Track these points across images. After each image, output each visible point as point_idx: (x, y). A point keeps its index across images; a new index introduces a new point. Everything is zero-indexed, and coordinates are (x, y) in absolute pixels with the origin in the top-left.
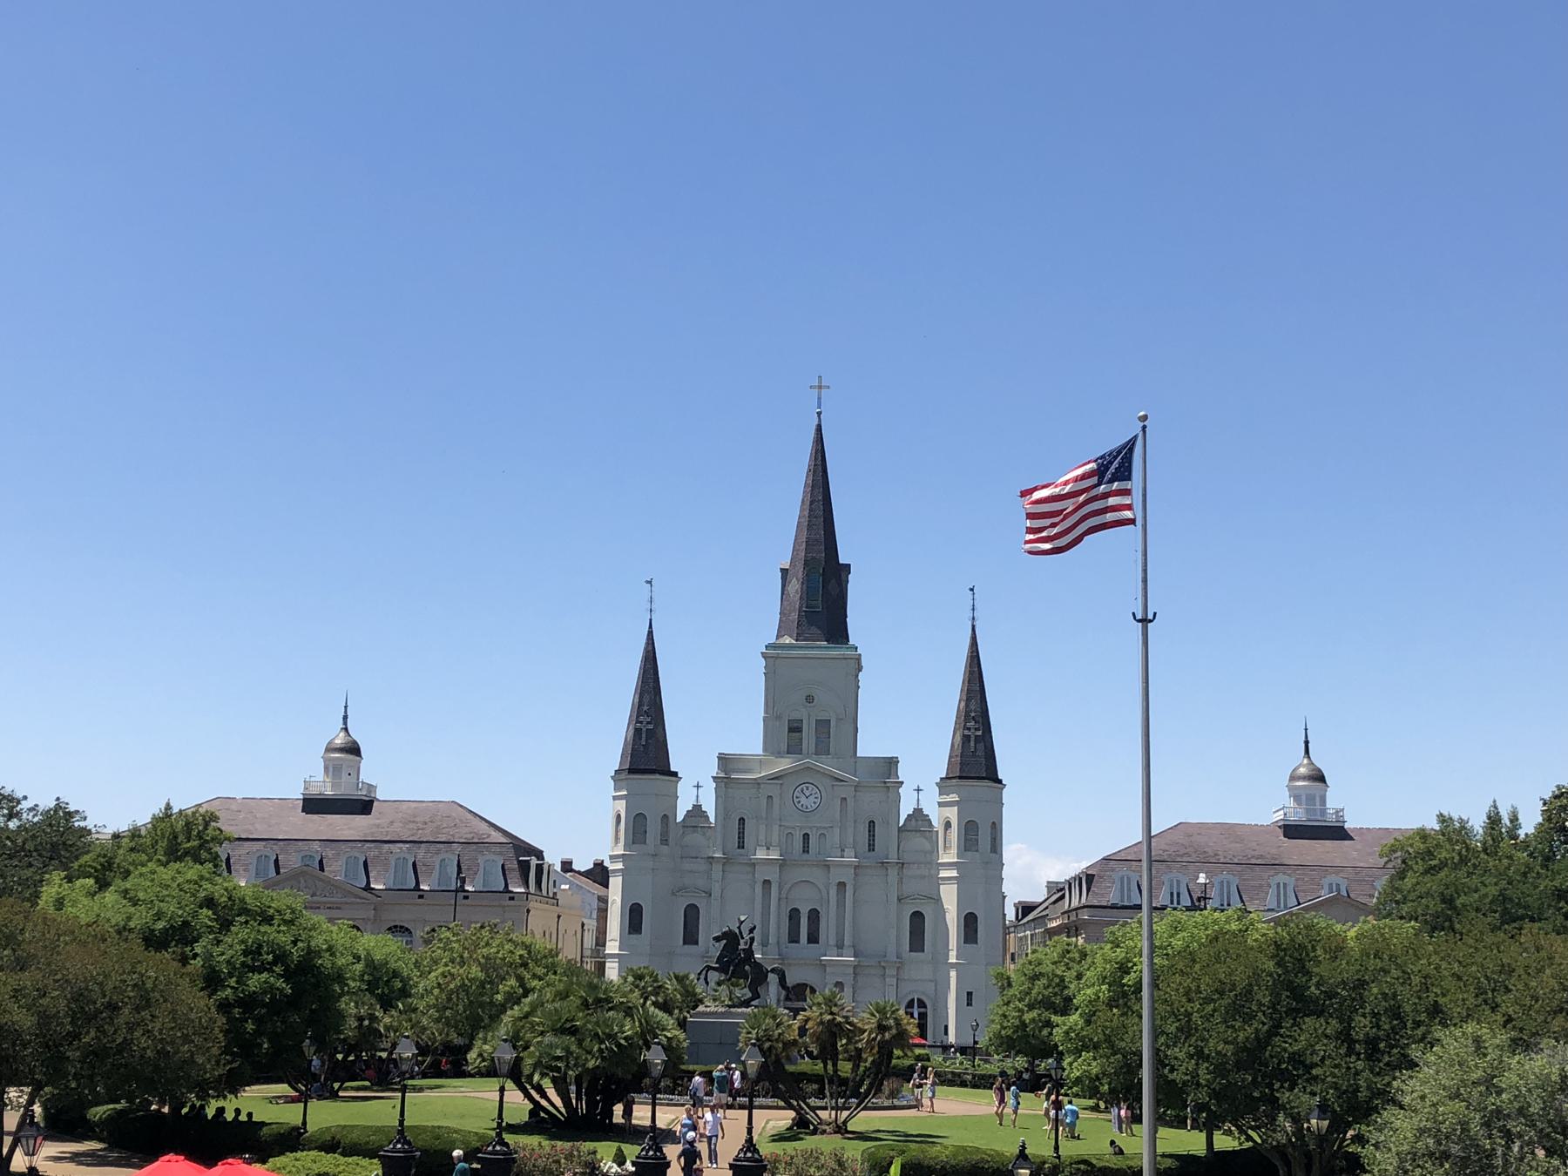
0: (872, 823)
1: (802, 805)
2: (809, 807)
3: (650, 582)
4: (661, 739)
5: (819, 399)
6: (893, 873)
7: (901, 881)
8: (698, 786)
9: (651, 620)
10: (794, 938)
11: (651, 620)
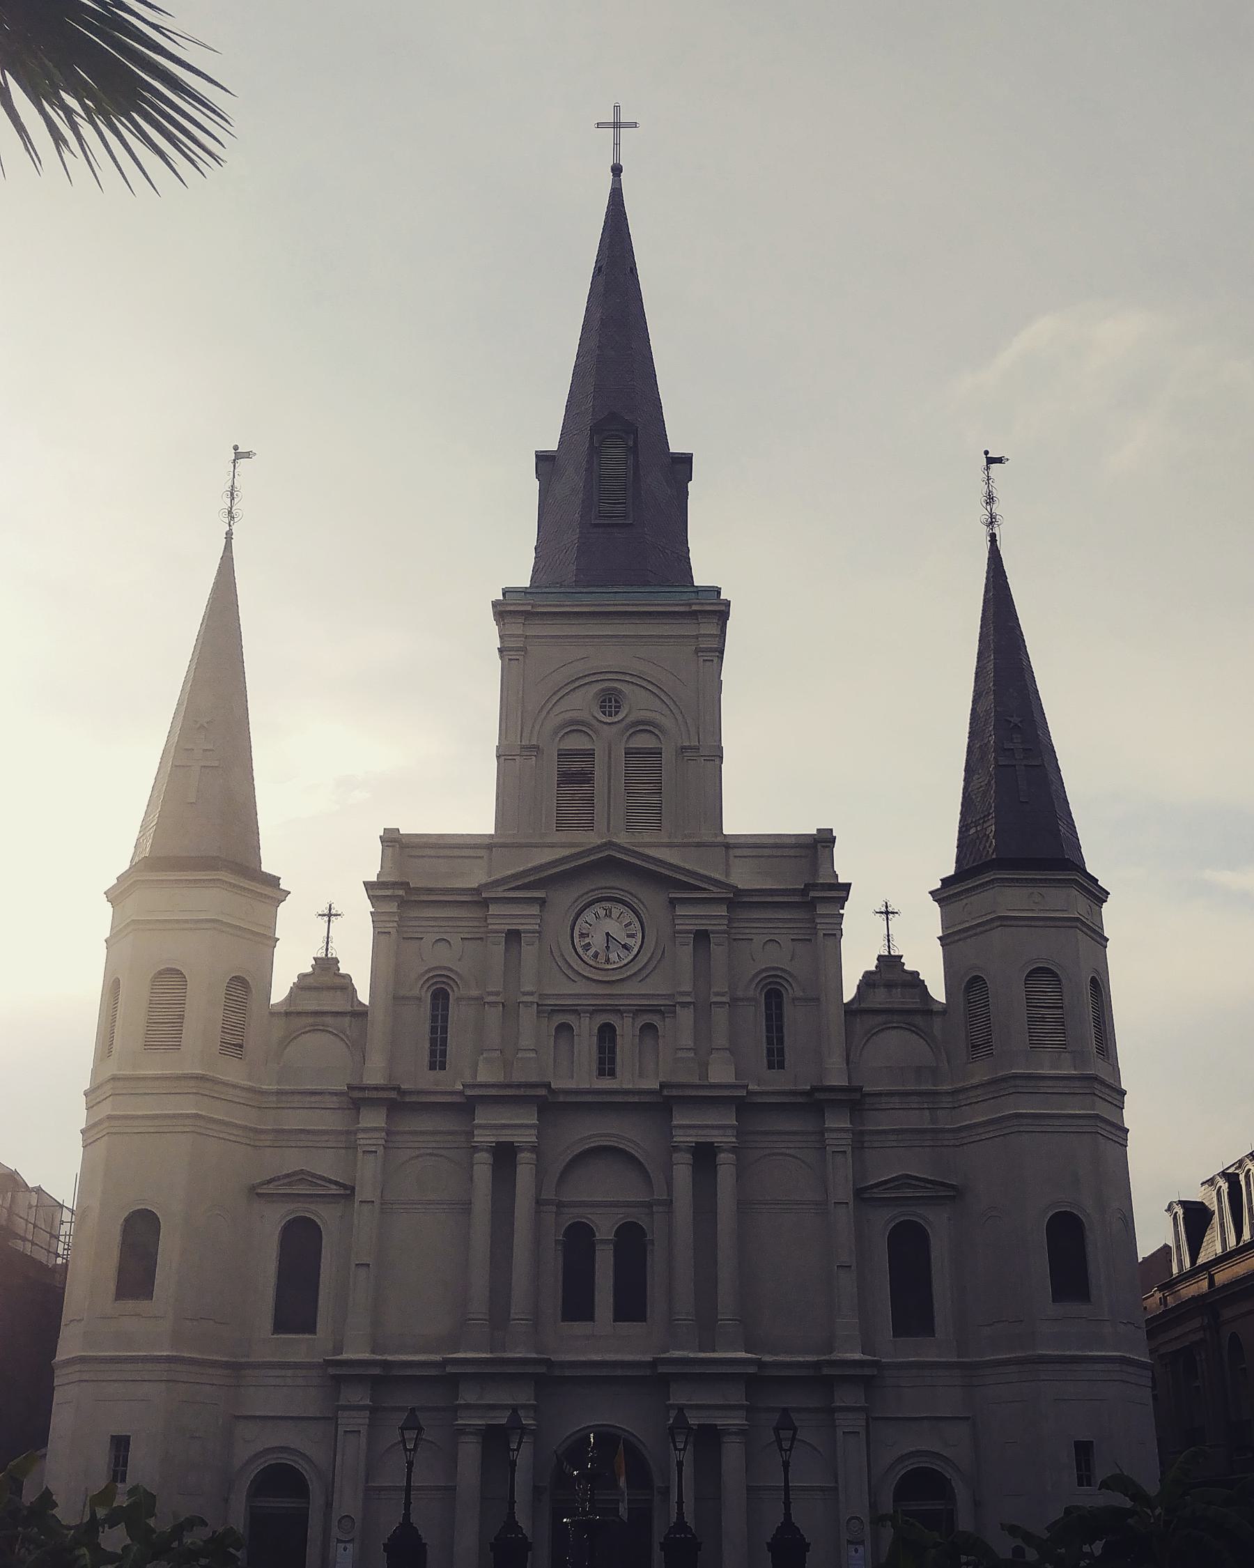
0: (774, 998)
5: (617, 144)
6: (837, 1122)
7: (859, 1142)
8: (330, 915)
9: (229, 536)
11: (229, 536)
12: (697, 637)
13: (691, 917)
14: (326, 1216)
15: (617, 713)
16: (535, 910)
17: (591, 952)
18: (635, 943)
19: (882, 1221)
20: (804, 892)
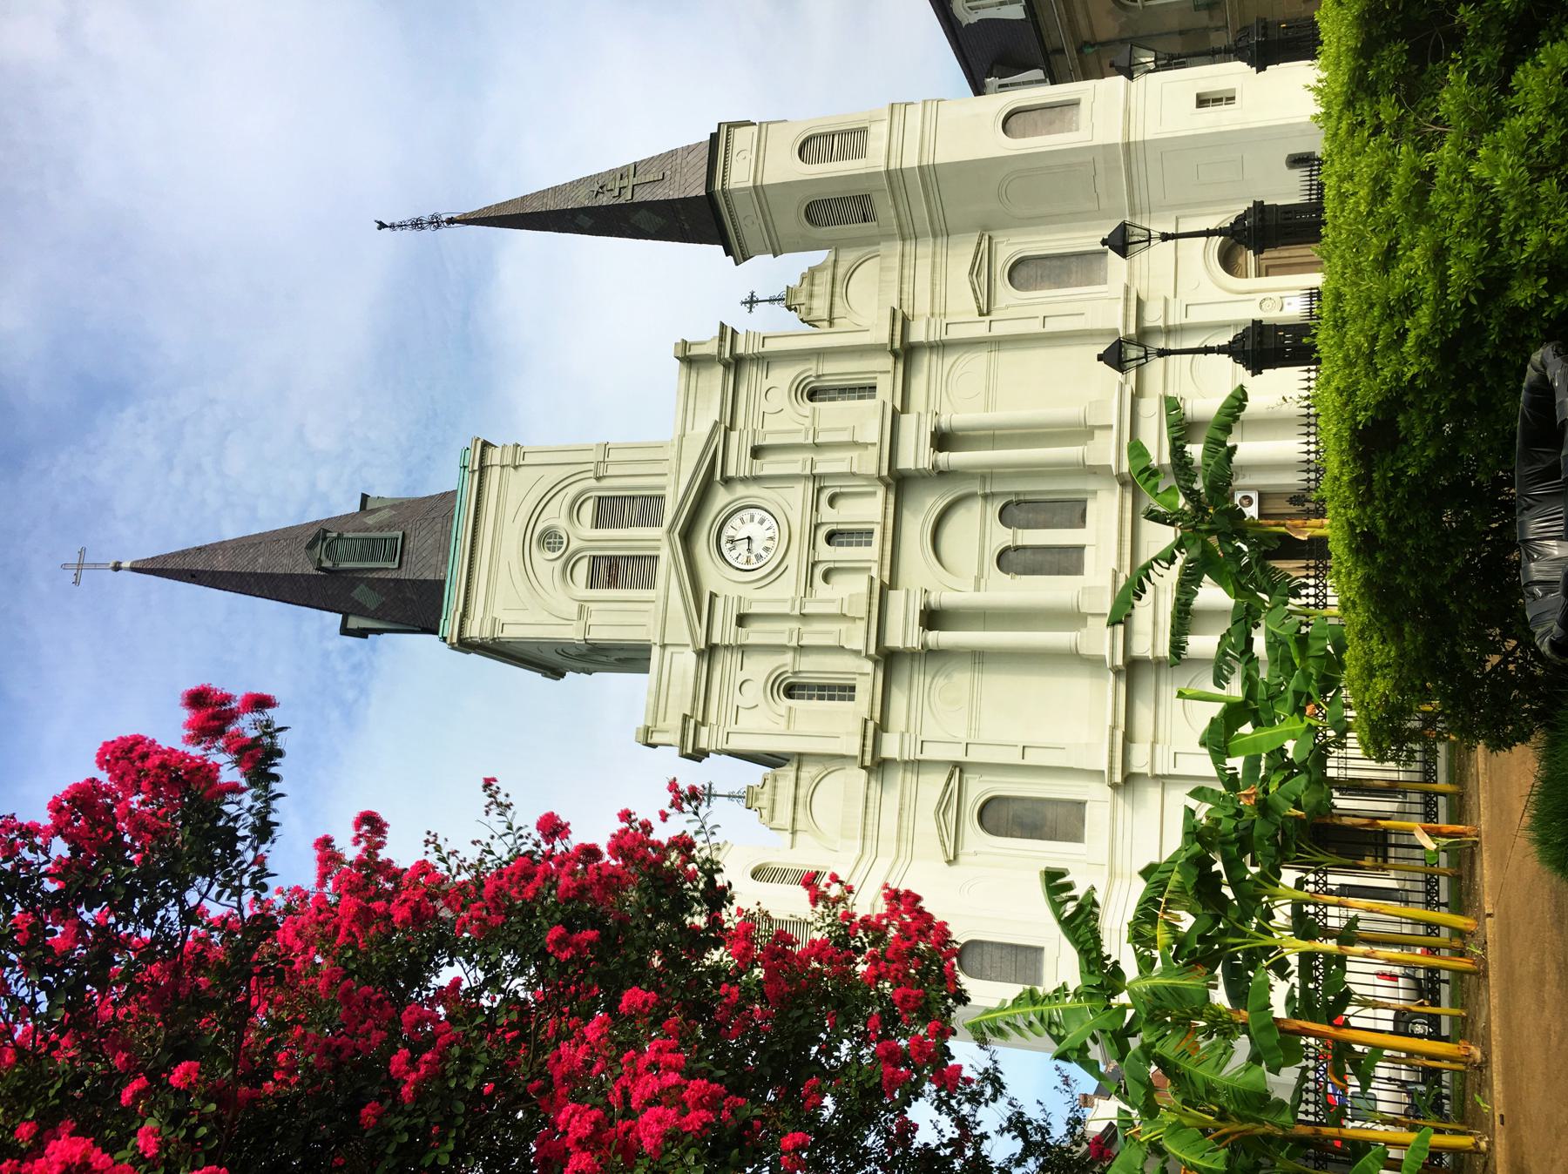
1: (767, 549)
2: (770, 533)
10: (1068, 561)
12: (502, 467)
13: (738, 463)
14: (978, 789)
15: (561, 537)
16: (719, 603)
17: (764, 554)
18: (759, 514)
19: (1005, 293)
20: (727, 366)
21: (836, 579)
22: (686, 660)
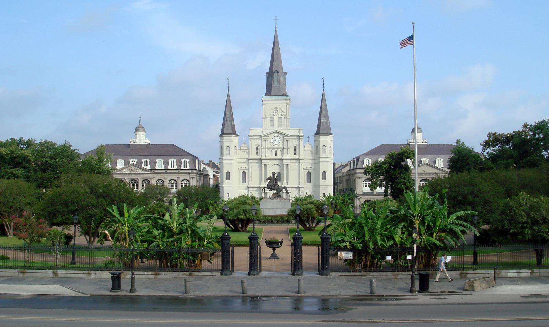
3: (228, 79)
4: (233, 125)
9: (228, 90)
11: (228, 90)
13: (285, 138)
14: (246, 171)
20: (299, 136)
21: (271, 152)
22: (260, 134)
